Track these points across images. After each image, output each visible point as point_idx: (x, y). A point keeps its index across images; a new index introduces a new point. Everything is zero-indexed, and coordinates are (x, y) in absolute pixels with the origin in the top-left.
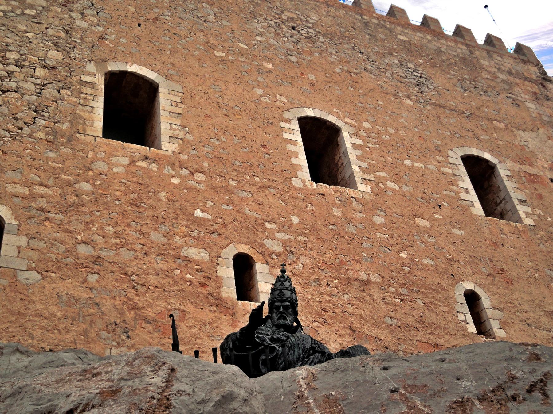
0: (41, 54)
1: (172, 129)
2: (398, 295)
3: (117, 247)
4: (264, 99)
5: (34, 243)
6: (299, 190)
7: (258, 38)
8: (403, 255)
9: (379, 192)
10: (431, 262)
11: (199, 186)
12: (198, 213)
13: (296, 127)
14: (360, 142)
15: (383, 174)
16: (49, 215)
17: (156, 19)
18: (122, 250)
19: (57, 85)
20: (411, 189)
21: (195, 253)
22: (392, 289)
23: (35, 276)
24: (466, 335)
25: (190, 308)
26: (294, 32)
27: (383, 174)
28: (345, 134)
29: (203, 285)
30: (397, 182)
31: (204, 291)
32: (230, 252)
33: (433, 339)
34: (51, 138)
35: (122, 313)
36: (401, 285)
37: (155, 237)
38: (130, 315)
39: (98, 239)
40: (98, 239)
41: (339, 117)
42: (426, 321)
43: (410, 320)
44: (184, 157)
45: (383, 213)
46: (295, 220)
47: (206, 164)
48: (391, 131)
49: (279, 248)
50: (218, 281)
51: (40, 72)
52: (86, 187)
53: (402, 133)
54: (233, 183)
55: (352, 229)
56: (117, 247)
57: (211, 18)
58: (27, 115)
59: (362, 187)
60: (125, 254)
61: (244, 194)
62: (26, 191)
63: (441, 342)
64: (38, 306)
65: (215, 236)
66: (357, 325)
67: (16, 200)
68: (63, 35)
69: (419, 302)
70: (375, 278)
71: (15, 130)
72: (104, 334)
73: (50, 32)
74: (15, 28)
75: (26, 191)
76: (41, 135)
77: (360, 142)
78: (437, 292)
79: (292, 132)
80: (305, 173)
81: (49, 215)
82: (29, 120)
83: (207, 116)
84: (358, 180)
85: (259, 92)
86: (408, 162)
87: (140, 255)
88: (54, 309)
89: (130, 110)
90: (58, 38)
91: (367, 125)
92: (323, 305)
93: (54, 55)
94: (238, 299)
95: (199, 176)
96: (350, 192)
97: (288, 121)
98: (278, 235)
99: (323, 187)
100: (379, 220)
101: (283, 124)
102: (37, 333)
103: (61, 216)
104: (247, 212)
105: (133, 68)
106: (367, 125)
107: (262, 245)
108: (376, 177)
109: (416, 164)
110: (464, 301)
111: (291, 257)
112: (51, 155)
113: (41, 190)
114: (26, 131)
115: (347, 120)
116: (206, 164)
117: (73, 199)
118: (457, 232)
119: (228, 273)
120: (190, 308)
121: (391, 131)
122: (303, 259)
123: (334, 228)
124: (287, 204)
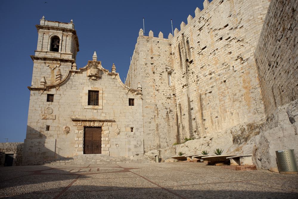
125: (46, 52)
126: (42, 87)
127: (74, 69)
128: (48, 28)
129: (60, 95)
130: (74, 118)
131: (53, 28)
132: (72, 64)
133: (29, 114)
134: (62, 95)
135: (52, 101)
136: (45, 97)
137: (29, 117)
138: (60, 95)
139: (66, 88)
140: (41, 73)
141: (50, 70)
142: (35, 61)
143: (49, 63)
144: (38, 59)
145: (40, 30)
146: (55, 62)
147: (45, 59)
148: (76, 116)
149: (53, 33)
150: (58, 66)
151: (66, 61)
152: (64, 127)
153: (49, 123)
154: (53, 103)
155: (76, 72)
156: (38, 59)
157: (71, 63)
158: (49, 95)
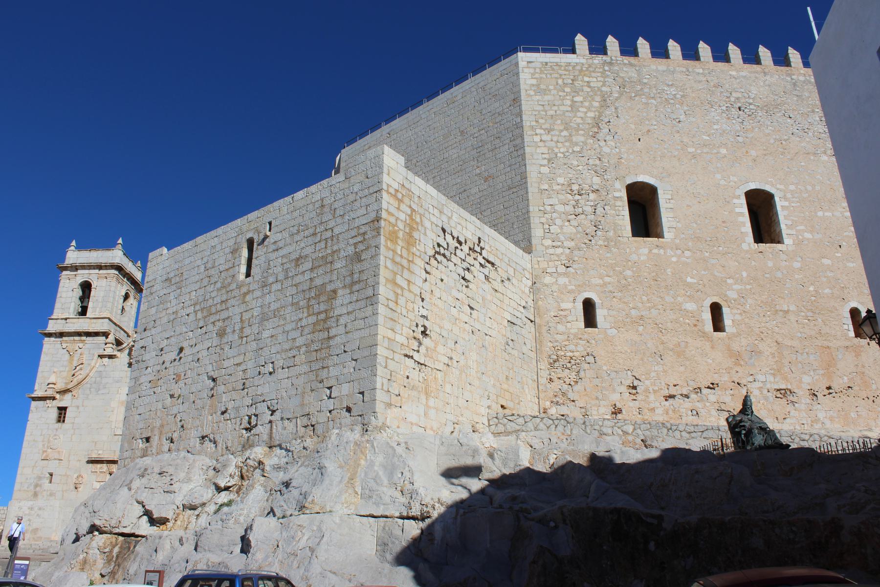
0: (589, 181)
1: (669, 221)
2: (806, 317)
3: (650, 309)
4: (722, 182)
5: (611, 313)
6: (747, 252)
7: (715, 127)
8: (811, 289)
9: (799, 243)
10: (830, 291)
11: (688, 261)
12: (689, 280)
13: (743, 201)
14: (786, 204)
15: (802, 227)
16: (615, 294)
17: (649, 131)
18: (652, 310)
19: (602, 203)
20: (820, 236)
21: (690, 306)
22: (803, 314)
23: (614, 331)
24: (848, 339)
25: (689, 340)
26: (741, 112)
27: (802, 227)
28: (777, 199)
29: (695, 325)
30: (811, 232)
31: (696, 329)
32: (707, 303)
33: (826, 343)
34: (606, 243)
35: (657, 347)
36: (808, 310)
37: (669, 299)
38: (661, 347)
39: (640, 305)
40: (640, 305)
41: (772, 185)
42: (822, 332)
43: (813, 333)
44: (677, 241)
45: (799, 259)
46: (745, 274)
47: (690, 244)
48: (809, 188)
49: (735, 296)
50: (703, 321)
51: (592, 196)
52: (629, 273)
53: (818, 188)
54: (707, 254)
55: (779, 275)
56: (650, 309)
57: (682, 118)
58: (591, 230)
59: (787, 240)
60: (654, 312)
61: (714, 261)
62: (601, 281)
63: (830, 345)
64: (619, 348)
65: (699, 293)
66: (780, 340)
67: (598, 288)
68: (598, 162)
69: (820, 320)
70: (793, 308)
71: (588, 242)
72: (651, 359)
73: (591, 162)
74: (572, 164)
75: (601, 281)
76: (601, 242)
77: (786, 204)
78: (832, 312)
79: (741, 206)
80: (750, 238)
81: (615, 294)
82: (593, 233)
83: (688, 206)
84: (784, 236)
85: (718, 176)
86: (820, 214)
87: (662, 311)
88: (626, 348)
89: (643, 211)
90: (596, 166)
91: (792, 187)
92: (761, 330)
93: (596, 180)
94: (715, 331)
95: (687, 253)
96: (779, 246)
97: (739, 197)
98: (735, 287)
99: (762, 246)
100: (797, 265)
101: (735, 201)
102: (621, 361)
103: (620, 294)
104: (716, 274)
105: (641, 178)
106: (792, 187)
107: (726, 296)
108: (797, 231)
109: (827, 214)
110: (849, 315)
111: (742, 300)
112: (608, 255)
113: (607, 279)
114: (593, 242)
115: (778, 186)
116: (690, 244)
117: (624, 282)
118: (851, 265)
119: (707, 316)
120: (689, 340)
121: (809, 188)
122: (749, 301)
123: (767, 276)
124: (739, 263)
125: (66, 319)
126: (50, 393)
127: (109, 351)
128: (75, 268)
129: (78, 407)
130: (94, 456)
131: (83, 267)
132: (107, 338)
133: (24, 451)
134: (81, 409)
135: (64, 421)
136: (55, 413)
137: (23, 456)
138: (78, 407)
139: (88, 392)
140: (53, 364)
141: (67, 356)
142: (46, 339)
143: (66, 342)
144: (50, 335)
145: (65, 273)
146: (77, 338)
147: (61, 335)
148: (100, 452)
149: (83, 275)
150: (81, 345)
151: (96, 334)
152: (75, 476)
153: (52, 466)
154: (64, 425)
155: (111, 357)
156: (50, 335)
157: (104, 338)
158: (60, 408)
